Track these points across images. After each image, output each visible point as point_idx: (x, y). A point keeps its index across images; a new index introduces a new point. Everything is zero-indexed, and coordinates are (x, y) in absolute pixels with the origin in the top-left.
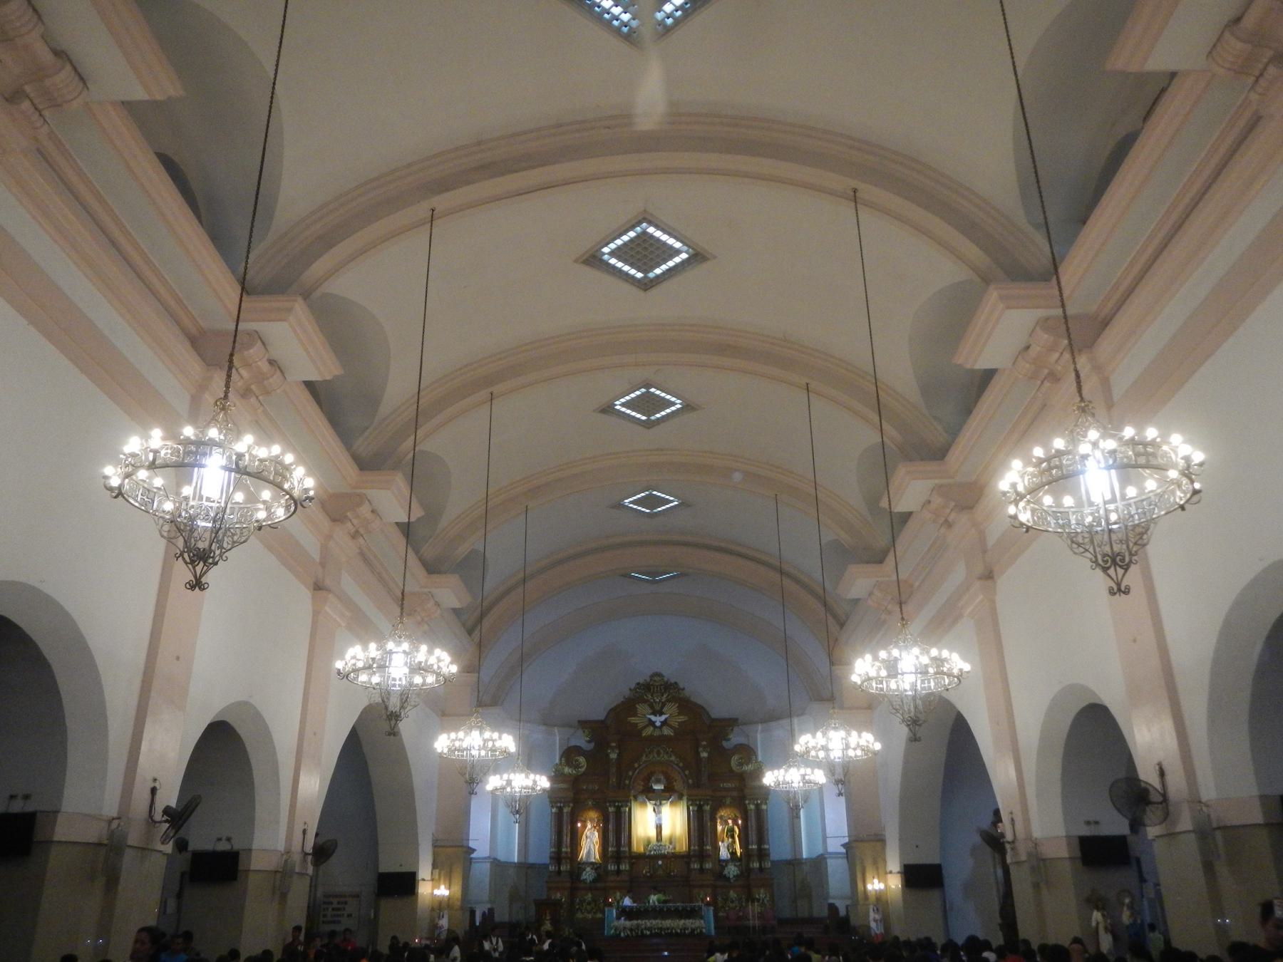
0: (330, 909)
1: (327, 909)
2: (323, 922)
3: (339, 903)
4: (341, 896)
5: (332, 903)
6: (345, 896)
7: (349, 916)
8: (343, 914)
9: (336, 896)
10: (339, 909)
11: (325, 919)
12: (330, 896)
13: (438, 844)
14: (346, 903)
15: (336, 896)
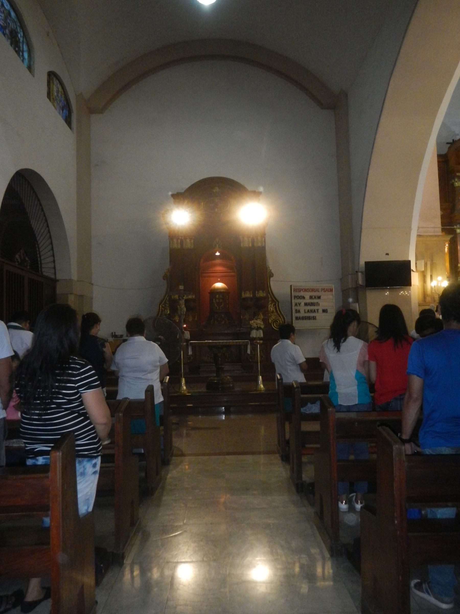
0: (303, 304)
1: (300, 304)
2: (297, 318)
3: (311, 297)
4: (313, 290)
5: (304, 298)
6: (317, 290)
7: (325, 311)
8: (318, 310)
9: (306, 290)
10: (312, 304)
11: (298, 315)
12: (300, 290)
13: (419, 234)
14: (319, 297)
15: (306, 290)
